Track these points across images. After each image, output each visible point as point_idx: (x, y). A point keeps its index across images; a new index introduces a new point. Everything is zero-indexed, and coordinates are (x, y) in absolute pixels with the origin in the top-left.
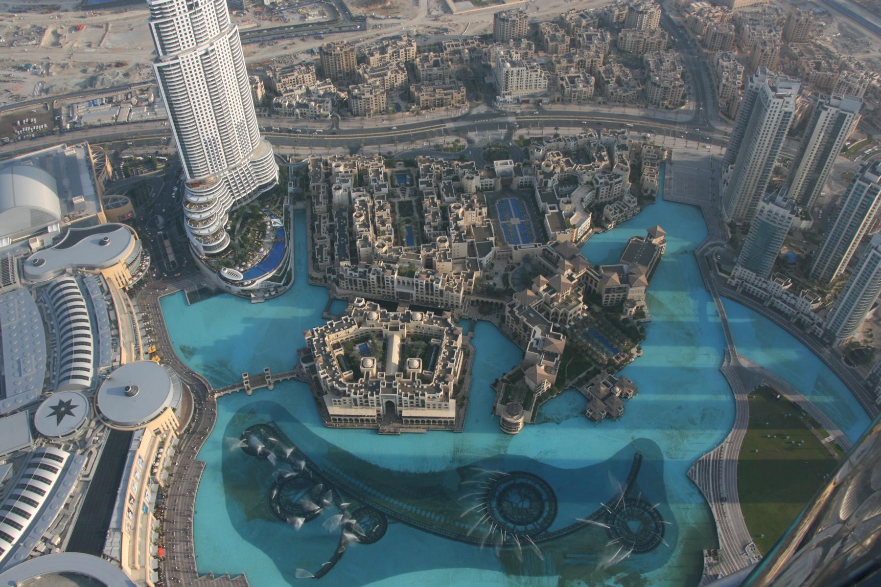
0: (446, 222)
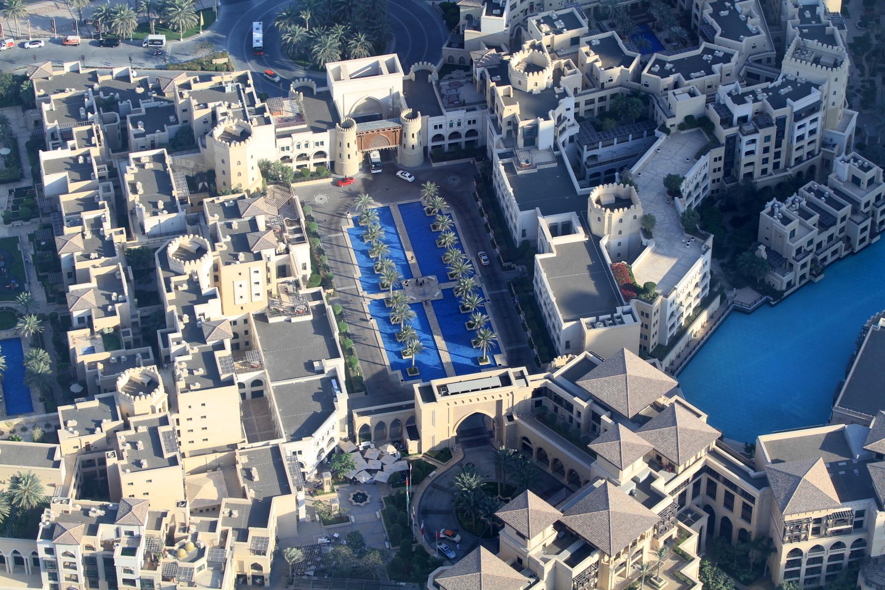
0: (149, 310)
